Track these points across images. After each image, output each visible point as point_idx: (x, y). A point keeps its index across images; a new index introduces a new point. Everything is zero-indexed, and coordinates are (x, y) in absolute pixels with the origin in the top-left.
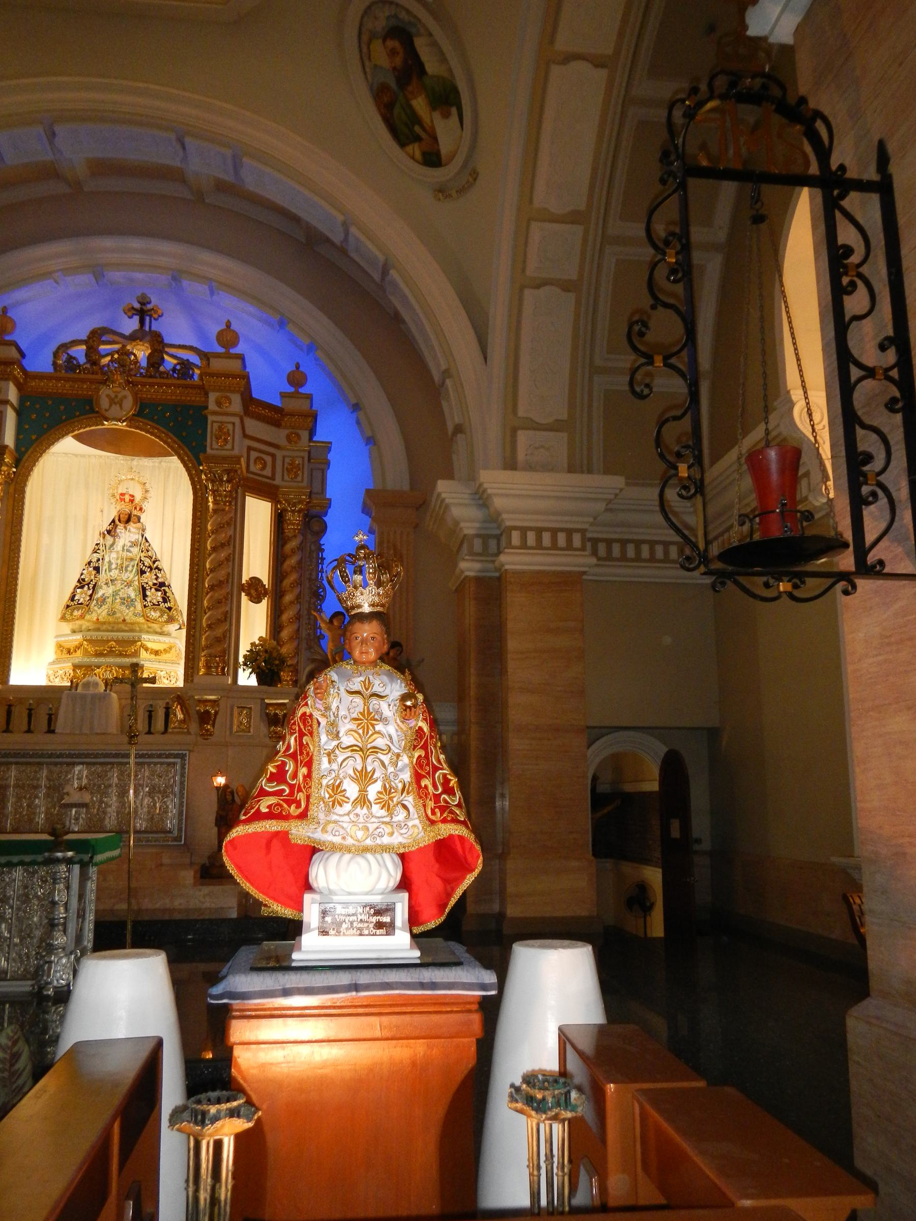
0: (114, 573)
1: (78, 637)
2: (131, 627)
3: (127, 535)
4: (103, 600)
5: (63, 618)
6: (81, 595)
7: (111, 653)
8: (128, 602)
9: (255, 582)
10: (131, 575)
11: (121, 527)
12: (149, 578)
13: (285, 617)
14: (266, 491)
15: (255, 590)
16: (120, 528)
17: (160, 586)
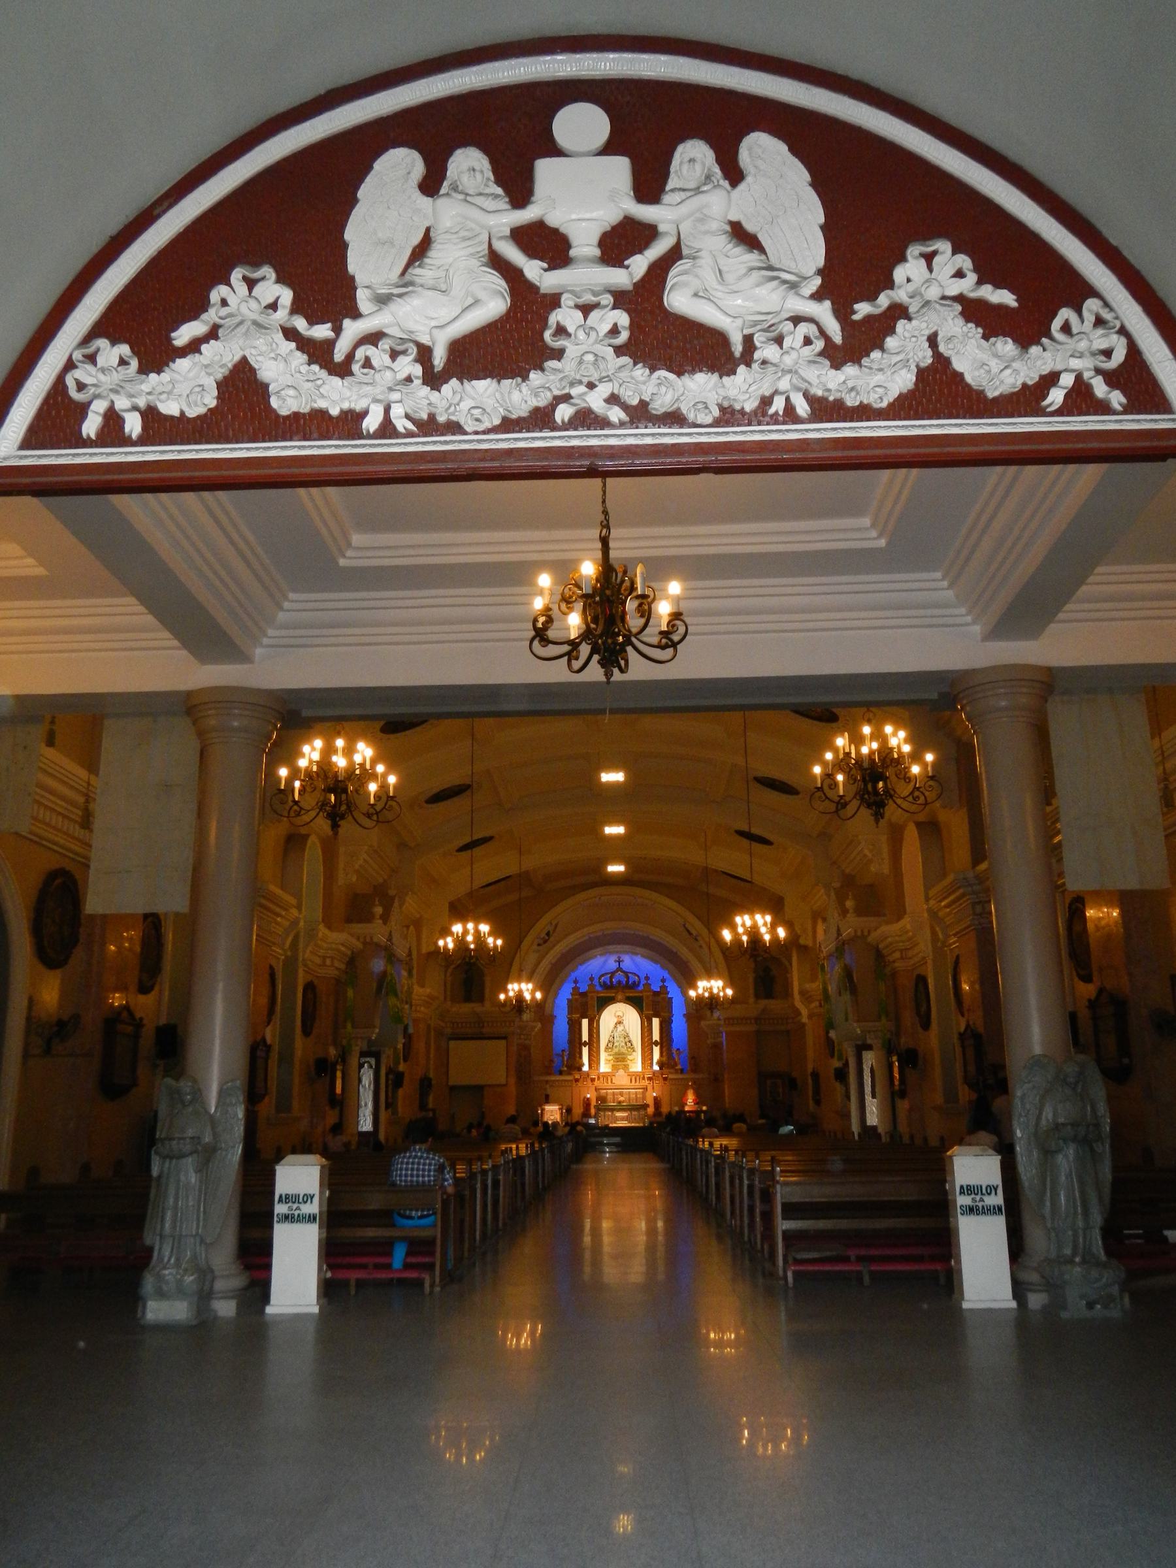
0: (618, 1039)
1: (611, 1057)
2: (623, 1054)
3: (620, 1028)
4: (616, 1047)
5: (605, 1051)
6: (610, 1045)
7: (620, 1061)
8: (622, 1047)
9: (656, 1041)
10: (622, 1039)
11: (618, 1026)
12: (627, 1039)
13: (664, 1049)
14: (656, 1016)
15: (656, 1043)
16: (618, 1026)
17: (630, 1041)
